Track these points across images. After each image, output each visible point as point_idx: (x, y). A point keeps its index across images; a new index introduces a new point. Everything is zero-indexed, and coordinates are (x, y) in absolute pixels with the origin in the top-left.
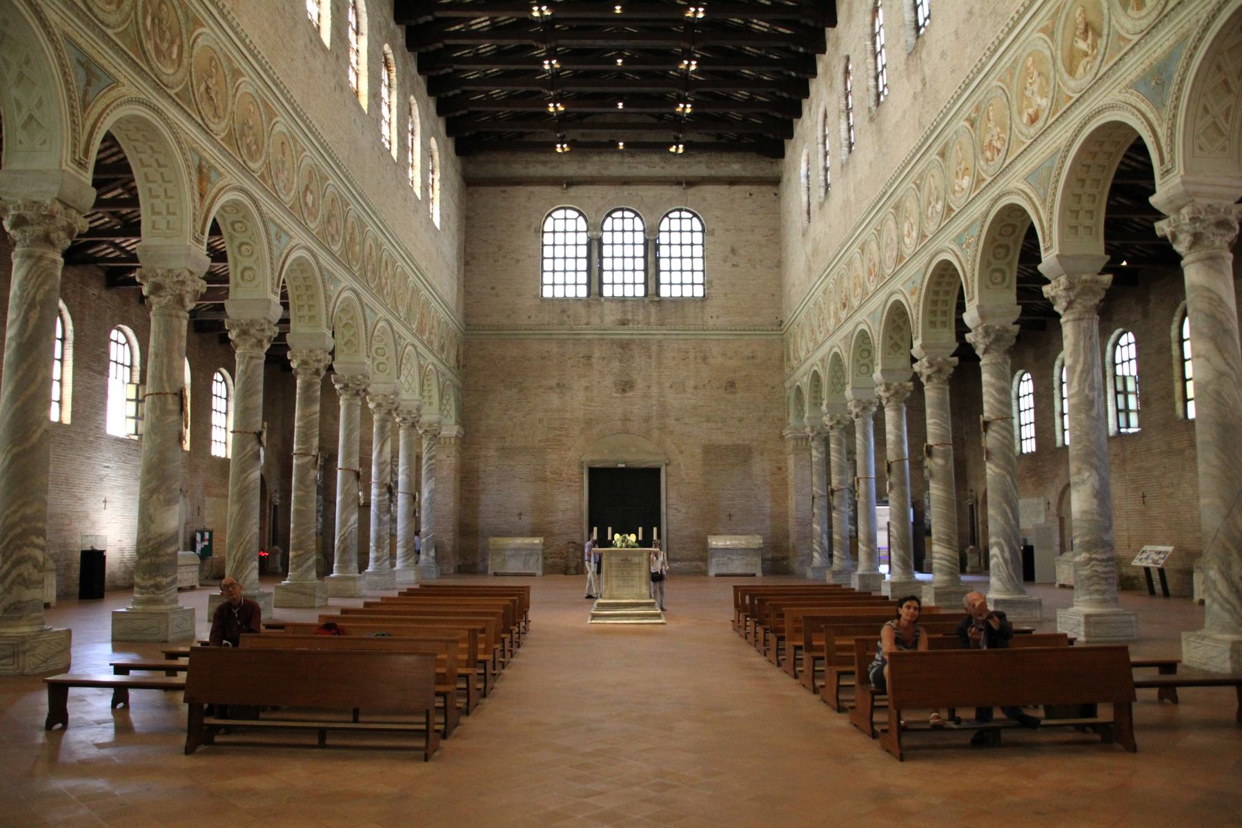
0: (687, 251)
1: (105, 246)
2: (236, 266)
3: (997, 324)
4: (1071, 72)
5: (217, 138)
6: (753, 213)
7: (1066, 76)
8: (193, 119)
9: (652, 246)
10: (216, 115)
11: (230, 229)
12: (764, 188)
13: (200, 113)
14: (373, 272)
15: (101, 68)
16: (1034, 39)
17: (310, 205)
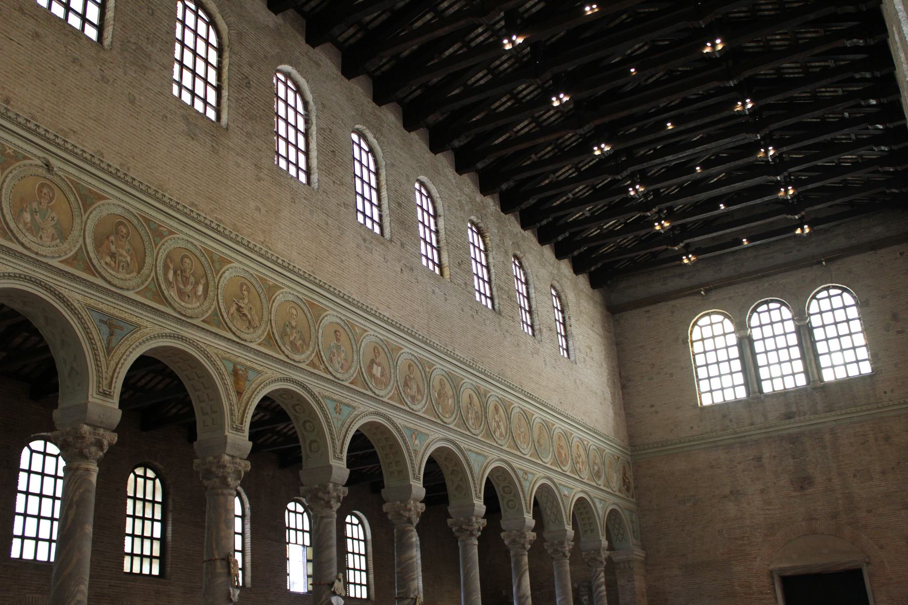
1: (269, 435)
9: (805, 333)
17: (379, 375)
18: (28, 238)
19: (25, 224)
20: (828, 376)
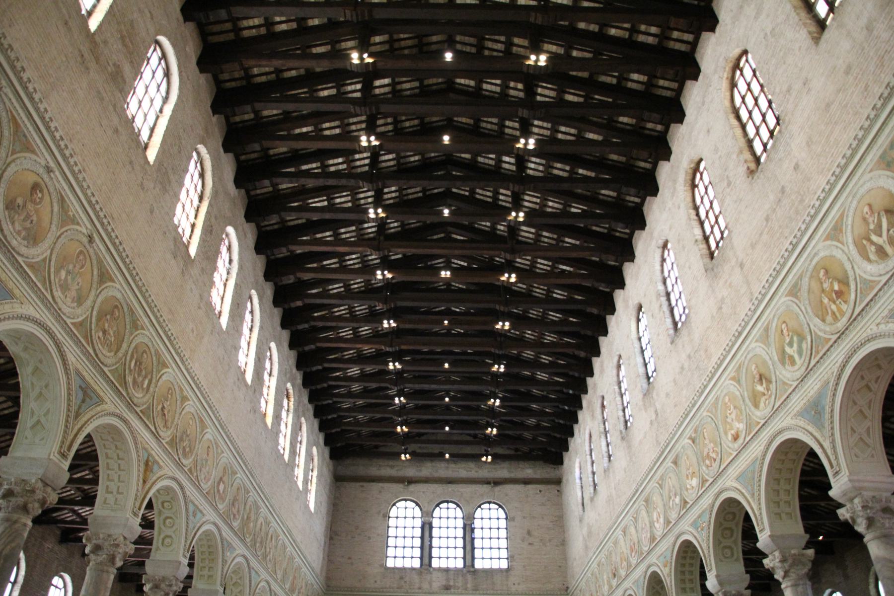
1: (66, 511)
2: (160, 534)
4: (756, 406)
5: (164, 442)
6: (543, 504)
7: (753, 408)
8: (149, 428)
9: (468, 529)
10: (166, 426)
11: (160, 506)
12: (549, 486)
13: (154, 424)
14: (261, 543)
15: (94, 391)
16: (727, 385)
17: (221, 491)
18: (58, 294)
19: (60, 280)
20: (478, 564)
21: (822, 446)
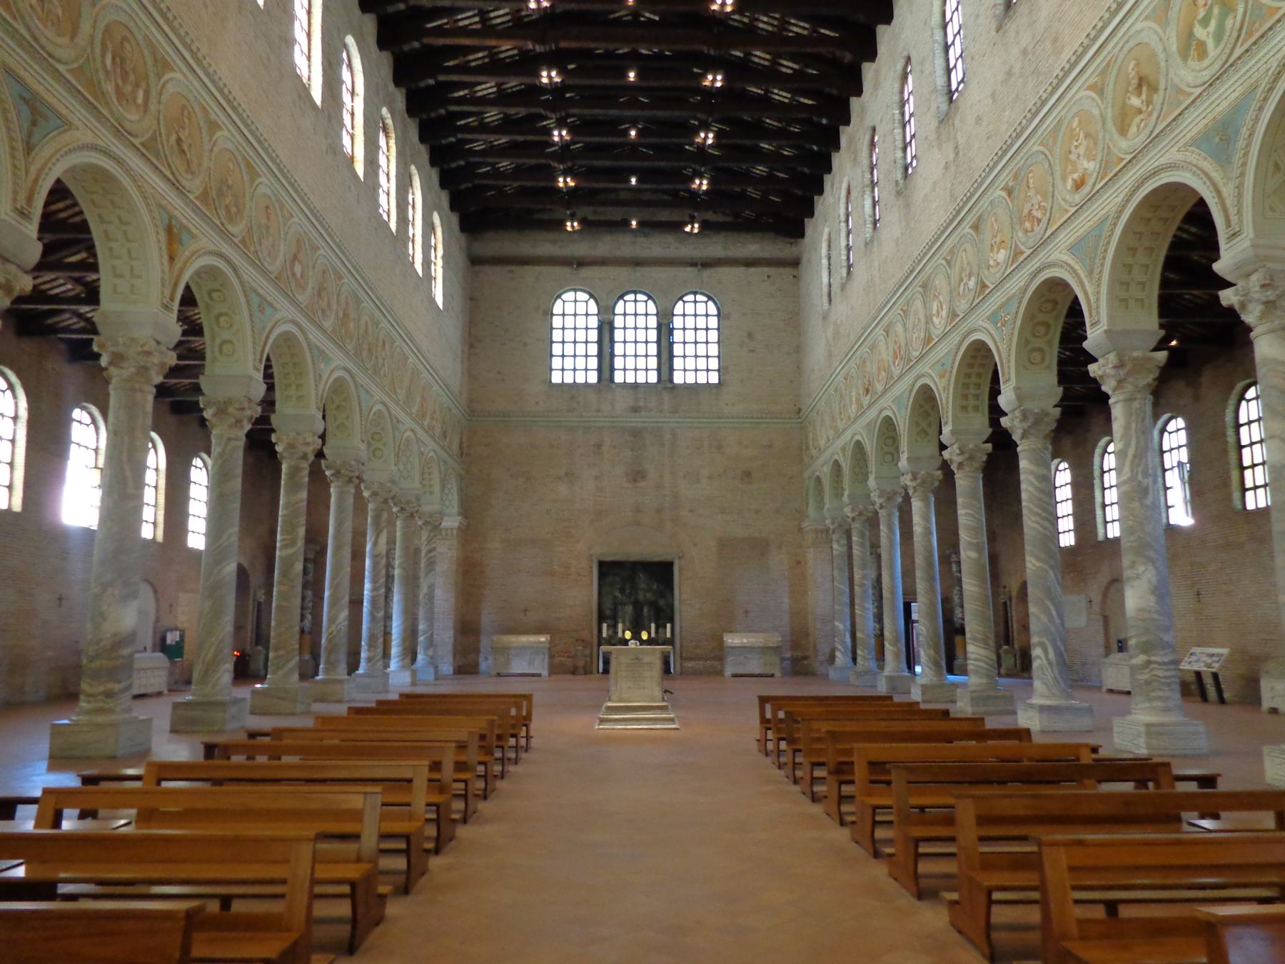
0: (701, 336)
2: (213, 339)
3: (1035, 406)
4: (1123, 131)
5: (191, 197)
7: (1116, 136)
9: (665, 330)
11: (207, 299)
12: (781, 270)
13: (169, 166)
14: (369, 350)
15: (50, 107)
16: (1082, 96)
17: (298, 275)
21: (1218, 192)
